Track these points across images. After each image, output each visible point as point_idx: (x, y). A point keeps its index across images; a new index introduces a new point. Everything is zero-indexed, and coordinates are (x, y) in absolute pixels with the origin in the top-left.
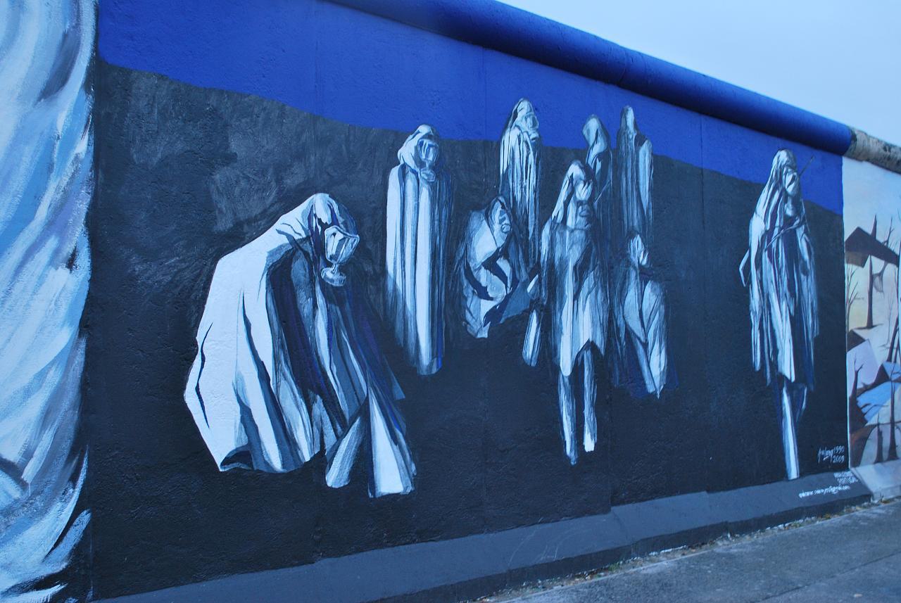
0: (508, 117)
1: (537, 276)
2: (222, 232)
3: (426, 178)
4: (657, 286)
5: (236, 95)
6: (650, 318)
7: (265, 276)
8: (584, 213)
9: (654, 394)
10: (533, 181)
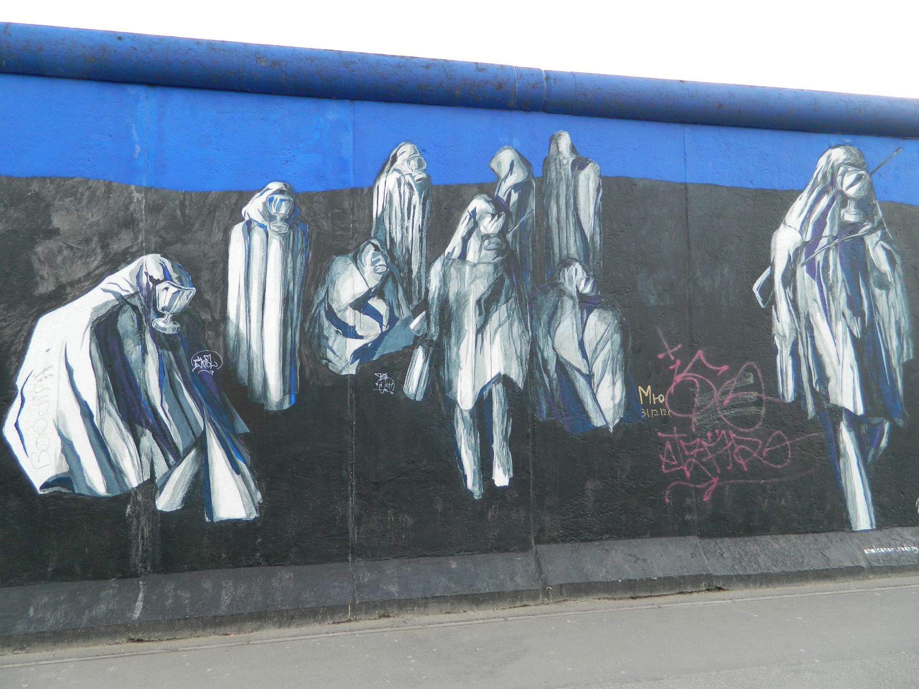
0: (387, 161)
1: (424, 313)
2: (43, 294)
3: (277, 230)
4: (609, 316)
5: (59, 179)
6: (596, 347)
7: (89, 328)
8: (492, 246)
9: (605, 429)
10: (418, 221)
